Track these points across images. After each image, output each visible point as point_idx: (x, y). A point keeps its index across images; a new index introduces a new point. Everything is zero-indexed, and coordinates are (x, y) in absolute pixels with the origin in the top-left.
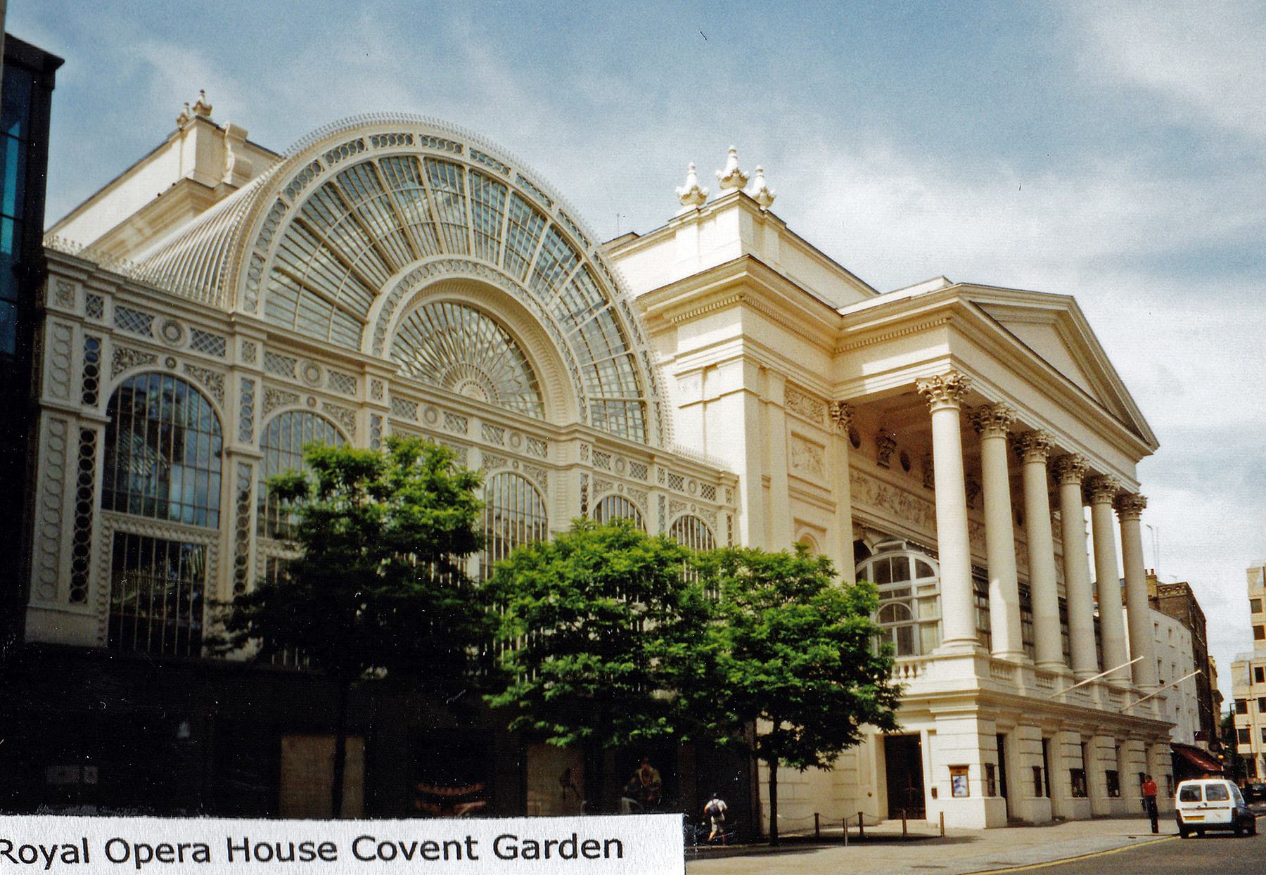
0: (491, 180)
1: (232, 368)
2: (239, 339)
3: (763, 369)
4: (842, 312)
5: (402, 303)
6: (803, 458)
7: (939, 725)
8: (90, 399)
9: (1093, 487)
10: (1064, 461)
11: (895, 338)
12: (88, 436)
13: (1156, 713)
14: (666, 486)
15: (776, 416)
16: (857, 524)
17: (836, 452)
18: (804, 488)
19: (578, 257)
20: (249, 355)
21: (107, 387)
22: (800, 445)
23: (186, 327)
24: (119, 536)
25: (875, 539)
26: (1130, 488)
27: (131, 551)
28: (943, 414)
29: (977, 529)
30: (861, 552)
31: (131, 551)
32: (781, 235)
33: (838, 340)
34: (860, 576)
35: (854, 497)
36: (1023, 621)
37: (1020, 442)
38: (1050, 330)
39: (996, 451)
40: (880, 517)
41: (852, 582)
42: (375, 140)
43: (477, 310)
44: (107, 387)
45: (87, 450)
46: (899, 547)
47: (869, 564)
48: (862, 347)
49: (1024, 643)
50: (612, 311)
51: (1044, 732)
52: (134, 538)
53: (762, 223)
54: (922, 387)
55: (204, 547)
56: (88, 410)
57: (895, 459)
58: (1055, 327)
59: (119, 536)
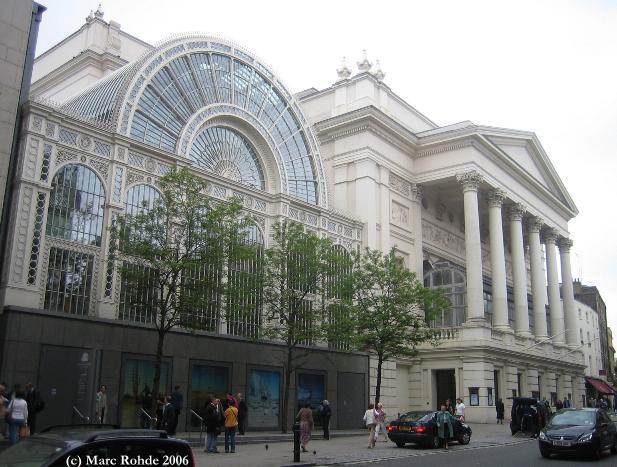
0: (243, 64)
1: (112, 162)
2: (117, 147)
3: (378, 165)
4: (419, 136)
5: (197, 128)
6: (398, 214)
7: (466, 366)
8: (44, 177)
9: (547, 234)
10: (530, 220)
11: (453, 149)
12: (41, 197)
13: (577, 360)
14: (326, 228)
15: (385, 191)
16: (425, 251)
17: (415, 213)
18: (398, 231)
19: (285, 105)
20: (121, 155)
21: (53, 170)
22: (396, 206)
23: (92, 140)
24: (53, 249)
25: (435, 260)
26: (565, 235)
27: (59, 258)
28: (470, 193)
29: (487, 254)
30: (426, 266)
31: (59, 258)
32: (389, 95)
33: (416, 150)
34: (426, 281)
35: (424, 236)
36: (509, 308)
37: (508, 209)
38: (523, 149)
39: (497, 214)
40: (438, 248)
41: (422, 282)
42: (189, 45)
43: (233, 131)
44: (53, 170)
45: (41, 204)
46: (446, 265)
47: (430, 274)
48: (430, 154)
49: (510, 320)
50: (302, 132)
51: (519, 369)
52: (59, 251)
53: (379, 88)
54: (459, 179)
55: (91, 257)
56: (43, 183)
57: (445, 216)
58: (526, 147)
59: (53, 249)
